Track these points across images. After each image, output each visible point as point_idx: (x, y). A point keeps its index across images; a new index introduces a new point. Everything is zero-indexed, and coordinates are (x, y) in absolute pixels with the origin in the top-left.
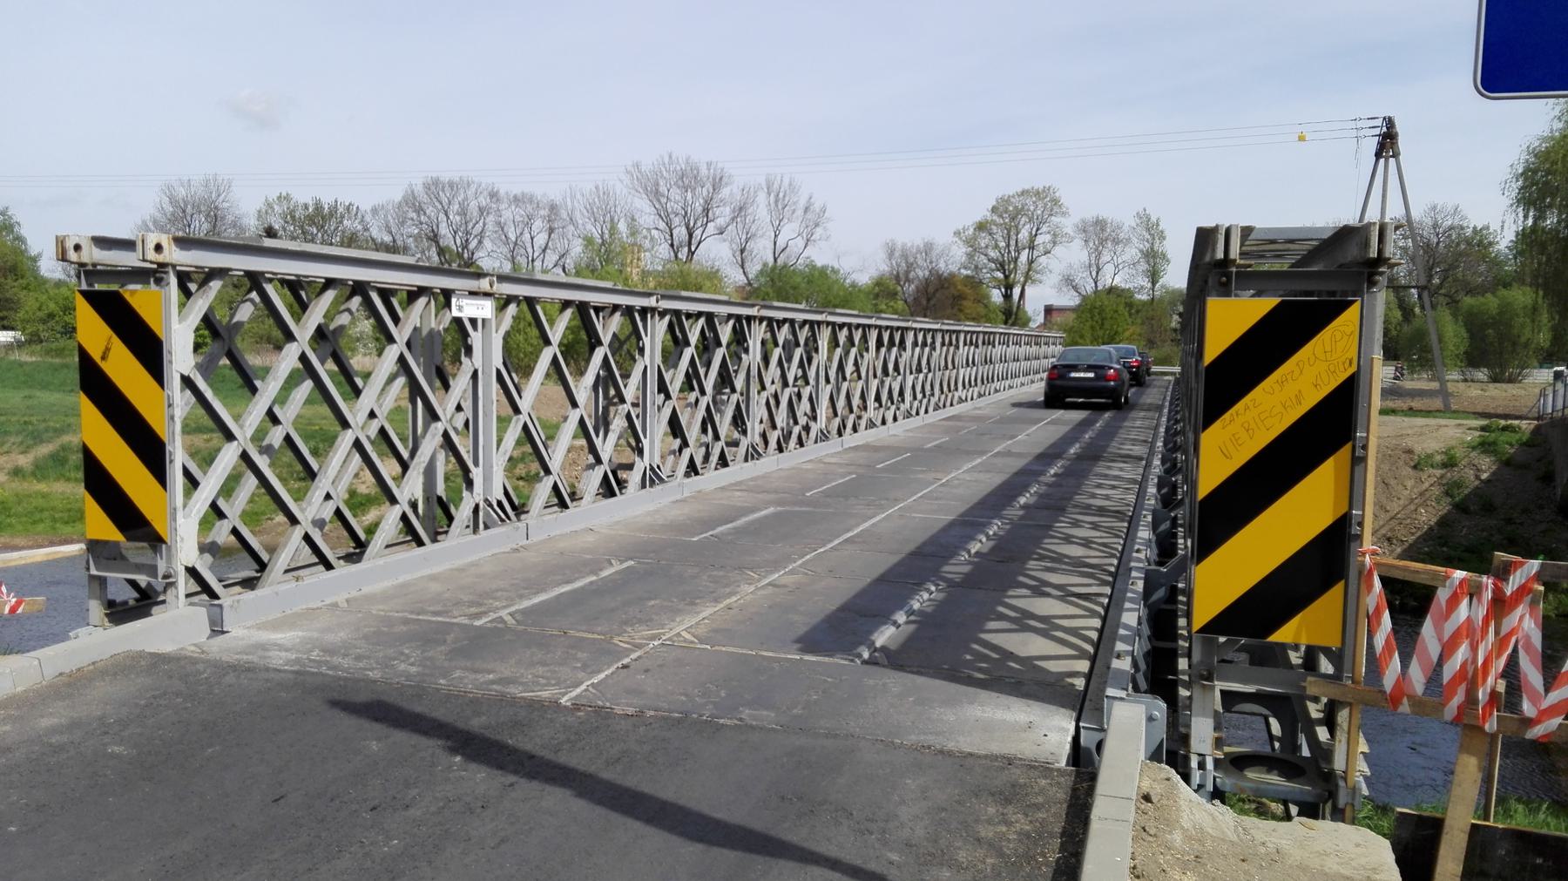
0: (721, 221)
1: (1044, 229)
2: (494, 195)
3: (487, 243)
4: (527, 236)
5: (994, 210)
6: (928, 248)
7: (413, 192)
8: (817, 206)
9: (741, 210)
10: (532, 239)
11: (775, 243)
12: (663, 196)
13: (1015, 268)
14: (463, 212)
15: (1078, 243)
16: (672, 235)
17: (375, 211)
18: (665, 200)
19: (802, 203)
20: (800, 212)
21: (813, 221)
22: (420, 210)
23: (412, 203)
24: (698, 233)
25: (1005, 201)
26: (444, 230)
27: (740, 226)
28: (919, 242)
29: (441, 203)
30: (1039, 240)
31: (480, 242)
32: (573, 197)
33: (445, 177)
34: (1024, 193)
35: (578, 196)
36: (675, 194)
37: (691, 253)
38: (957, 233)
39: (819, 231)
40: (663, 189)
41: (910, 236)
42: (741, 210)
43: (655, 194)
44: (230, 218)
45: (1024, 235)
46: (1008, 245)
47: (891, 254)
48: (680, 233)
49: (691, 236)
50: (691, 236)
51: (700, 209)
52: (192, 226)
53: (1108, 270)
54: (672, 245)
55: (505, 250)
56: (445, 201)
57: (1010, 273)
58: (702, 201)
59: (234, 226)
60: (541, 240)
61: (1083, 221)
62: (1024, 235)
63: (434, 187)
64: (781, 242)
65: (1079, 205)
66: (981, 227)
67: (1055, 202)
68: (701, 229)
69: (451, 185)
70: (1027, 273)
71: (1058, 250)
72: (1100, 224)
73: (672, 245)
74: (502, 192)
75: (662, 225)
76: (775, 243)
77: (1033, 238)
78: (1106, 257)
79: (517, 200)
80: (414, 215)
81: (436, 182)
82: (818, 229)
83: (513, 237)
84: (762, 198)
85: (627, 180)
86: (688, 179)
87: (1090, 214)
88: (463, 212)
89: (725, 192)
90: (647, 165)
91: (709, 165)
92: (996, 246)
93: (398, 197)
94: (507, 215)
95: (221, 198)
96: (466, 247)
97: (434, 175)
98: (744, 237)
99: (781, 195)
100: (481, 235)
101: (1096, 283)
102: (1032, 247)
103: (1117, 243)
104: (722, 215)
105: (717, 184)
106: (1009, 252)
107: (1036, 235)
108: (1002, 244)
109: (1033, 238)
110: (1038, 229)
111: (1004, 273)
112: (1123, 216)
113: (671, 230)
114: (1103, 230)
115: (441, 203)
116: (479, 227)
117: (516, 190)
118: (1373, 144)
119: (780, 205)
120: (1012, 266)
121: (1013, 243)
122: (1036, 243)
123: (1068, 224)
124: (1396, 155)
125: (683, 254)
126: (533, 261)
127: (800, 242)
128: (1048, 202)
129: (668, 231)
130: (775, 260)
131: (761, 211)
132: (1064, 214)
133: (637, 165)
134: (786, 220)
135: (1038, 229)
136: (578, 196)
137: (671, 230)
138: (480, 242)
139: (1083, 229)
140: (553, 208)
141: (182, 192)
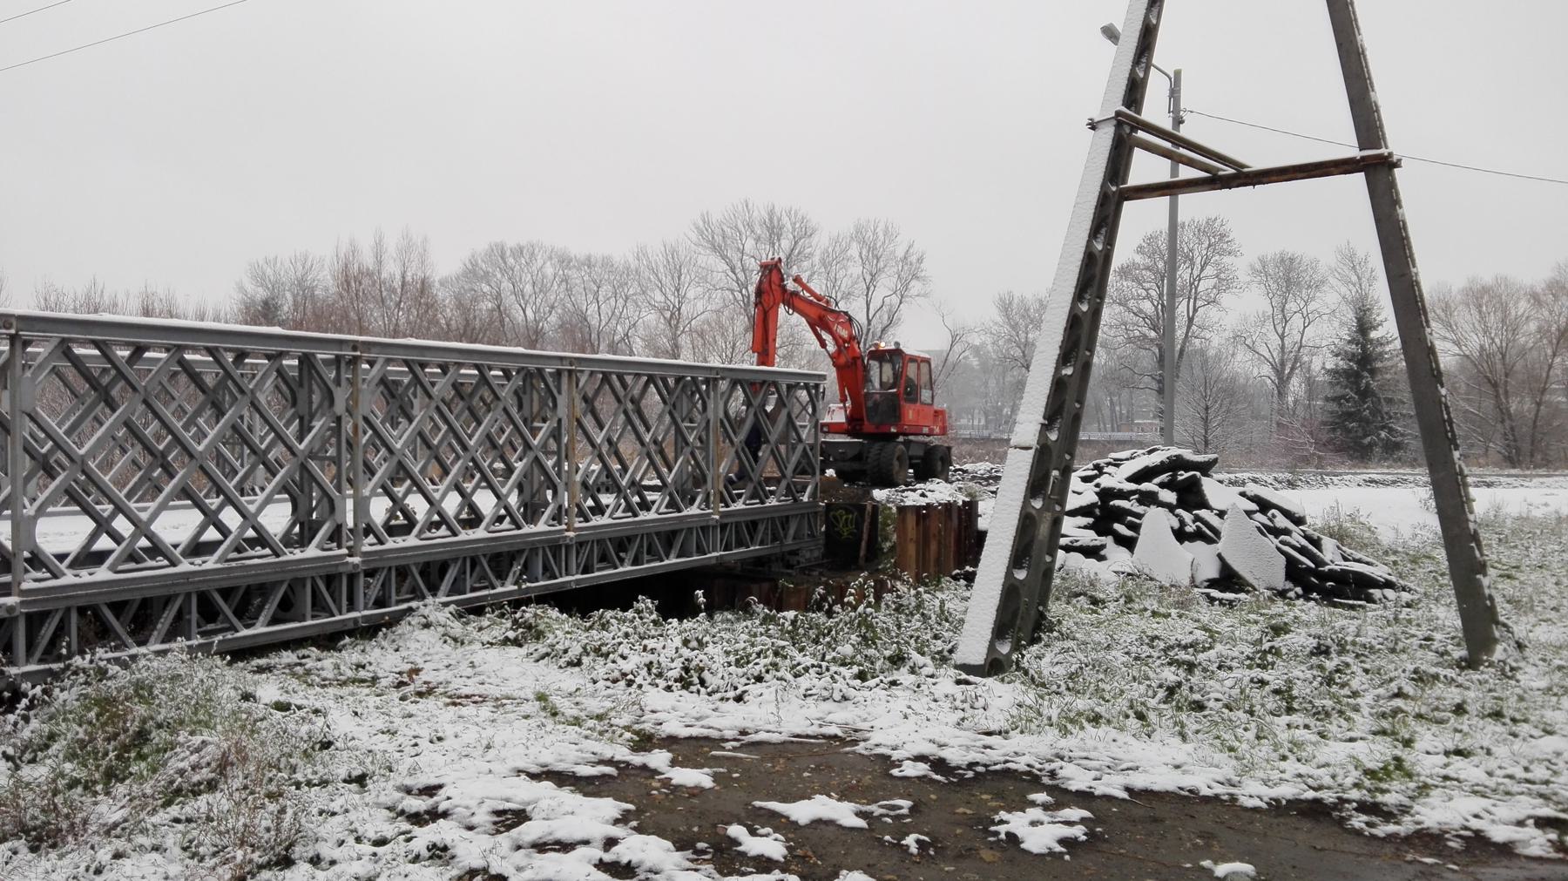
1: (1209, 270)
4: (595, 306)
5: (1140, 250)
8: (914, 259)
19: (900, 253)
33: (511, 243)
39: (916, 287)
47: (1006, 307)
53: (1297, 322)
63: (499, 254)
71: (1225, 299)
78: (1291, 306)
79: (588, 263)
82: (913, 283)
84: (854, 251)
87: (1272, 249)
90: (716, 217)
92: (1148, 297)
101: (1282, 340)
119: (873, 256)
122: (1199, 289)
123: (1240, 266)
127: (895, 299)
139: (1262, 270)
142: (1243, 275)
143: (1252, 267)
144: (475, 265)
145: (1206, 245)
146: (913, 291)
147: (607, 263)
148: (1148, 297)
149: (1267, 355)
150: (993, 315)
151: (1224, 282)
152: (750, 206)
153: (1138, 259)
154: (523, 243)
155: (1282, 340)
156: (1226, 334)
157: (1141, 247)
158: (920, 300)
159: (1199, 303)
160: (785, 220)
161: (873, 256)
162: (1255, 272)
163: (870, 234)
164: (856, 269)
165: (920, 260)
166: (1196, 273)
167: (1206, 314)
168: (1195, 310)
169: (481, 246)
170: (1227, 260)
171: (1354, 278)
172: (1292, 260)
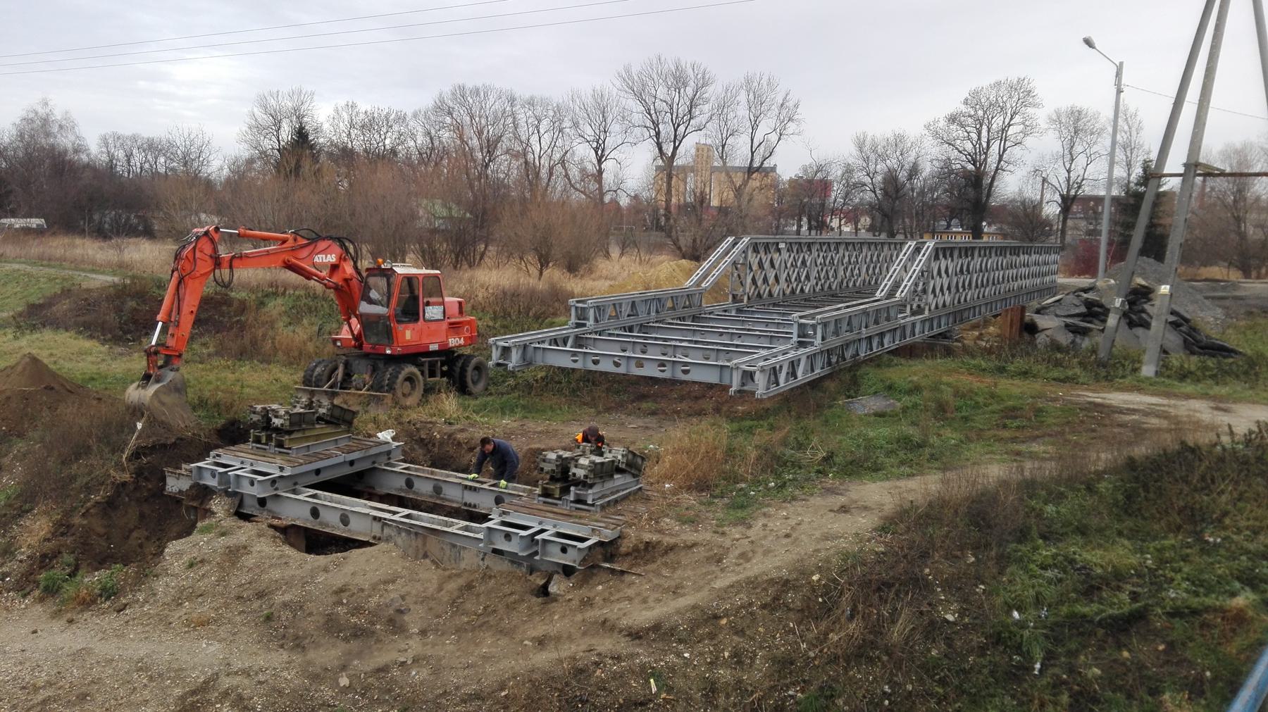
1: (1017, 119)
2: (512, 100)
4: (535, 137)
5: (966, 102)
6: (899, 140)
8: (790, 104)
9: (723, 107)
11: (752, 140)
13: (985, 159)
17: (415, 115)
21: (787, 115)
23: (442, 108)
24: (682, 128)
25: (976, 94)
28: (889, 135)
30: (1011, 131)
33: (470, 85)
34: (998, 84)
36: (662, 92)
37: (675, 148)
38: (927, 127)
39: (791, 127)
42: (723, 107)
46: (979, 138)
48: (666, 130)
49: (676, 130)
51: (683, 109)
53: (1081, 161)
57: (981, 165)
60: (546, 139)
62: (998, 123)
63: (461, 94)
64: (758, 137)
66: (953, 119)
71: (1029, 141)
76: (752, 140)
78: (1078, 148)
79: (531, 103)
81: (462, 88)
82: (790, 124)
84: (742, 97)
85: (618, 83)
87: (1065, 104)
92: (969, 138)
93: (431, 104)
94: (521, 117)
101: (1069, 171)
105: (704, 83)
106: (980, 144)
107: (1009, 125)
108: (974, 136)
110: (1011, 119)
111: (974, 164)
114: (1078, 120)
117: (527, 96)
120: (983, 157)
122: (1009, 133)
123: (1040, 116)
127: (774, 137)
128: (1022, 93)
130: (752, 153)
133: (628, 71)
135: (1011, 119)
139: (1057, 120)
140: (558, 109)
142: (1044, 125)
143: (1050, 118)
144: (442, 101)
145: (1015, 99)
146: (790, 131)
147: (545, 103)
148: (969, 138)
149: (1058, 186)
150: (854, 150)
151: (1028, 130)
152: (663, 59)
153: (963, 108)
154: (479, 84)
156: (1029, 169)
157: (967, 99)
158: (795, 138)
159: (1008, 144)
160: (690, 71)
162: (1052, 121)
163: (755, 84)
164: (742, 111)
165: (796, 106)
166: (1007, 121)
167: (1014, 153)
168: (1005, 150)
169: (447, 90)
170: (1030, 110)
172: (1080, 112)
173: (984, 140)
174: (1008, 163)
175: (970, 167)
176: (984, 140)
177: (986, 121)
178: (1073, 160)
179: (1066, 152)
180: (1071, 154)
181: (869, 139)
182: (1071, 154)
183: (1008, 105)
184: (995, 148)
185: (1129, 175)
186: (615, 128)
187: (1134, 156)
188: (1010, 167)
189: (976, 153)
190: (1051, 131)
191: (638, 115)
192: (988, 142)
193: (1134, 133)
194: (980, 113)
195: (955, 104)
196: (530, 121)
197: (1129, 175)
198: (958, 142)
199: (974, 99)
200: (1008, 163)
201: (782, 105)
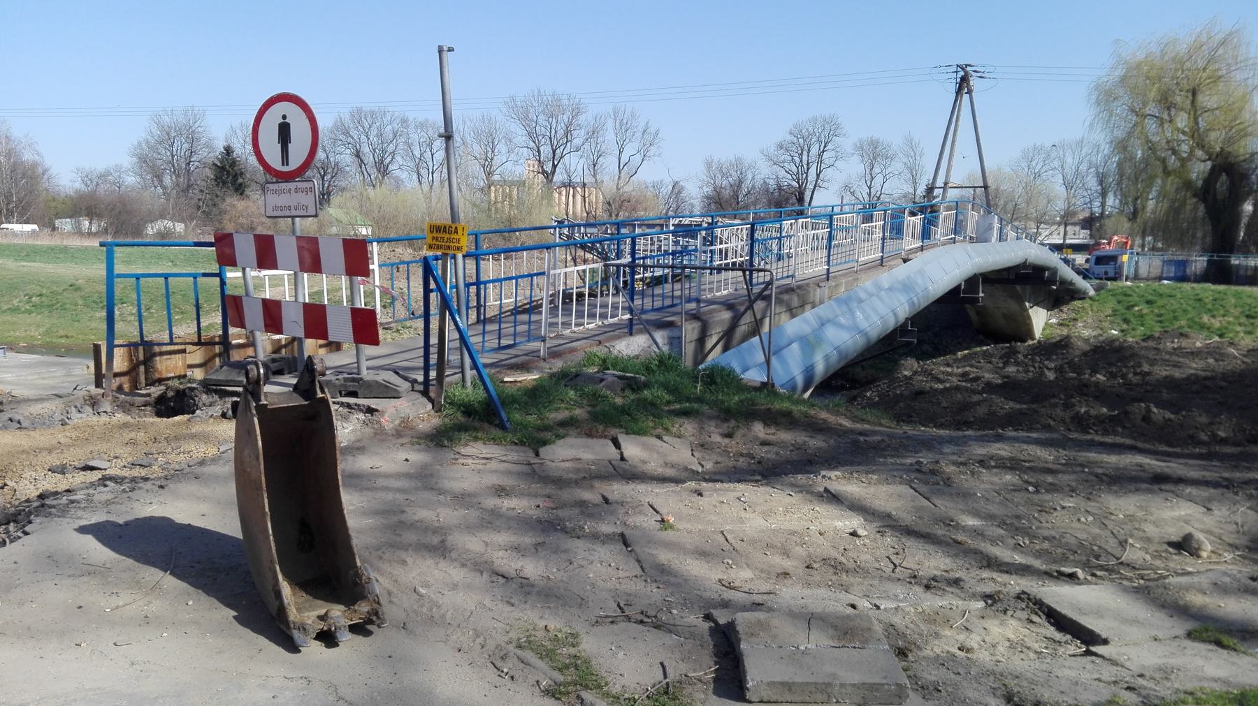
0: (578, 142)
1: (830, 146)
2: (404, 121)
3: (398, 159)
6: (738, 163)
7: (341, 119)
8: (652, 129)
10: (432, 155)
12: (532, 120)
14: (380, 135)
15: (856, 158)
16: (539, 151)
18: (534, 125)
19: (641, 126)
20: (639, 134)
21: (650, 141)
22: (347, 133)
26: (366, 149)
27: (593, 145)
29: (363, 128)
31: (393, 158)
32: (464, 123)
34: (815, 120)
35: (468, 123)
36: (542, 119)
37: (555, 167)
39: (653, 149)
40: (532, 116)
41: (725, 154)
42: (593, 134)
43: (525, 119)
44: (204, 140)
45: (815, 150)
46: (801, 161)
47: (709, 166)
48: (546, 150)
49: (554, 152)
50: (554, 152)
51: (561, 132)
52: (175, 145)
53: (879, 180)
54: (539, 161)
55: (412, 164)
56: (367, 126)
57: (803, 183)
58: (563, 125)
59: (207, 147)
61: (861, 141)
62: (815, 150)
64: (624, 159)
65: (854, 133)
67: (838, 126)
68: (562, 148)
69: (372, 113)
70: (817, 181)
71: (839, 164)
72: (874, 144)
73: (539, 161)
74: (411, 119)
75: (532, 145)
77: (821, 154)
78: (877, 170)
80: (341, 137)
81: (359, 111)
83: (417, 154)
84: (610, 124)
85: (504, 110)
86: (552, 109)
88: (380, 135)
89: (582, 119)
91: (569, 96)
92: (793, 160)
94: (414, 137)
95: (197, 125)
96: (382, 163)
97: (359, 105)
98: (596, 154)
99: (625, 121)
100: (393, 154)
101: (870, 189)
102: (820, 162)
103: (887, 158)
104: (579, 137)
105: (577, 112)
106: (802, 165)
107: (823, 151)
108: (797, 160)
109: (821, 154)
110: (825, 147)
111: (798, 182)
112: (892, 137)
113: (538, 148)
115: (363, 128)
116: (391, 148)
117: (421, 118)
118: (953, 88)
121: (805, 158)
123: (846, 143)
124: (970, 92)
125: (548, 167)
126: (432, 174)
127: (638, 158)
129: (535, 148)
131: (609, 137)
132: (844, 135)
134: (628, 140)
135: (825, 147)
136: (468, 123)
137: (538, 148)
138: (393, 158)
139: (860, 147)
141: (166, 120)
143: (855, 144)
155: (870, 189)
161: (624, 129)
167: (827, 173)
171: (912, 154)
173: (805, 162)
174: (824, 181)
175: (795, 184)
176: (805, 162)
177: (806, 147)
178: (873, 179)
179: (868, 172)
180: (871, 174)
181: (716, 160)
182: (871, 174)
183: (823, 137)
184: (813, 172)
185: (915, 190)
186: (501, 148)
187: (918, 175)
188: (825, 185)
189: (798, 173)
190: (855, 156)
191: (521, 138)
192: (808, 164)
193: (918, 158)
194: (801, 141)
195: (783, 135)
196: (422, 140)
197: (915, 190)
198: (786, 164)
199: (796, 132)
200: (824, 181)
201: (645, 131)
